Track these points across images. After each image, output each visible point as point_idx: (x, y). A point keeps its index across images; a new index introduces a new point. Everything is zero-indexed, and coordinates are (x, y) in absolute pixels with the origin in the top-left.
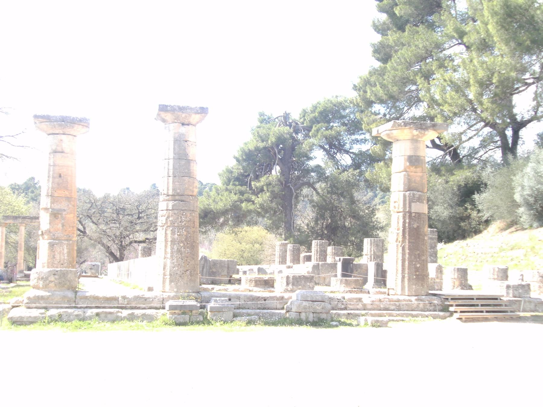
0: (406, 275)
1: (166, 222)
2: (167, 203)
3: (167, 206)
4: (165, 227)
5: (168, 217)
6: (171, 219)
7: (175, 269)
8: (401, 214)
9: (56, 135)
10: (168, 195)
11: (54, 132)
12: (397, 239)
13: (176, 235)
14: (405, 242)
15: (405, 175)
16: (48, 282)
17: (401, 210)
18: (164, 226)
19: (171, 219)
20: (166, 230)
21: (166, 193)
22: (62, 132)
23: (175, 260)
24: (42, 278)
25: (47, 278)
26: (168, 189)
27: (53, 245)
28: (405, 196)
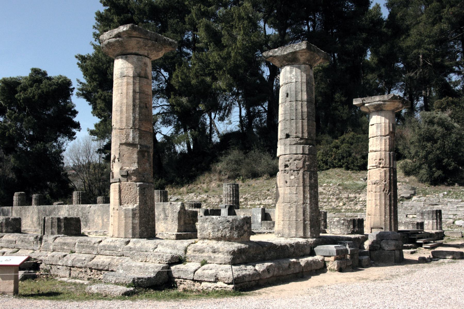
0: (392, 217)
1: (304, 167)
2: (303, 147)
3: (303, 150)
4: (301, 172)
5: (304, 162)
6: (307, 163)
7: (313, 214)
8: (387, 169)
9: (140, 57)
10: (301, 139)
11: (137, 52)
12: (384, 189)
13: (313, 180)
14: (391, 191)
15: (389, 139)
16: (242, 231)
17: (388, 166)
18: (299, 170)
19: (307, 163)
20: (304, 175)
21: (300, 135)
22: (146, 54)
23: (313, 206)
24: (237, 227)
25: (242, 227)
26: (303, 133)
27: (144, 189)
28: (390, 154)
